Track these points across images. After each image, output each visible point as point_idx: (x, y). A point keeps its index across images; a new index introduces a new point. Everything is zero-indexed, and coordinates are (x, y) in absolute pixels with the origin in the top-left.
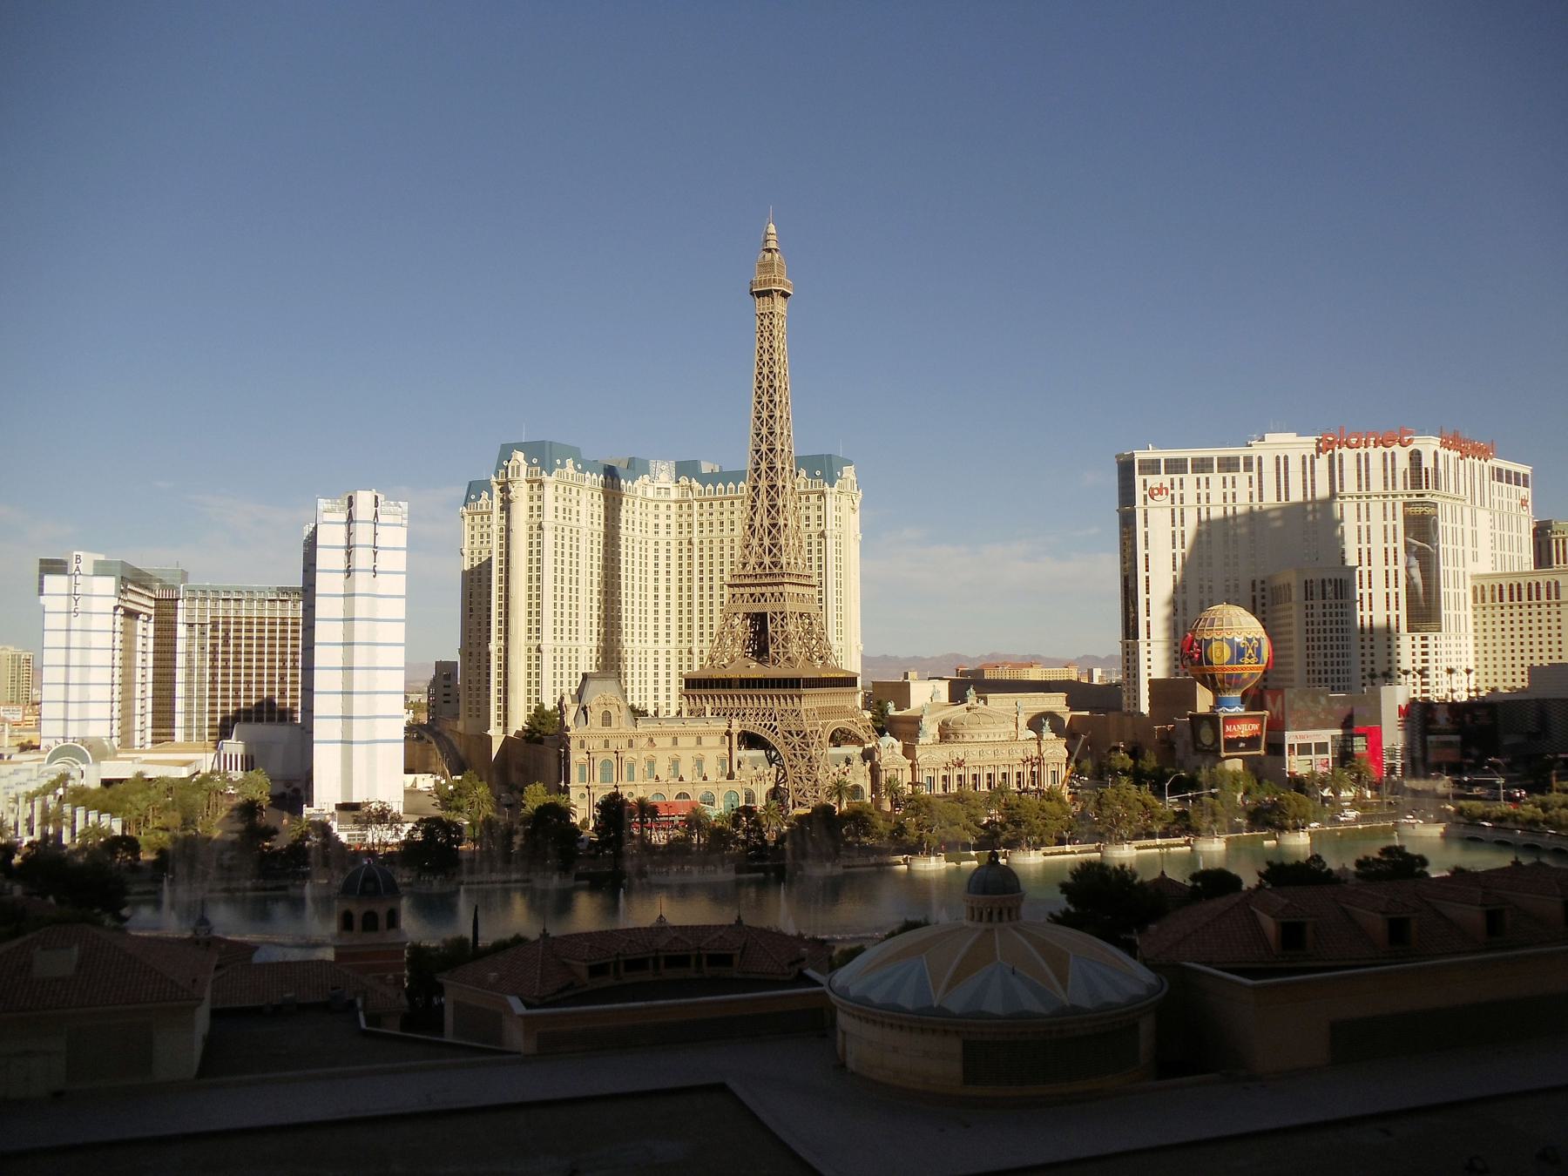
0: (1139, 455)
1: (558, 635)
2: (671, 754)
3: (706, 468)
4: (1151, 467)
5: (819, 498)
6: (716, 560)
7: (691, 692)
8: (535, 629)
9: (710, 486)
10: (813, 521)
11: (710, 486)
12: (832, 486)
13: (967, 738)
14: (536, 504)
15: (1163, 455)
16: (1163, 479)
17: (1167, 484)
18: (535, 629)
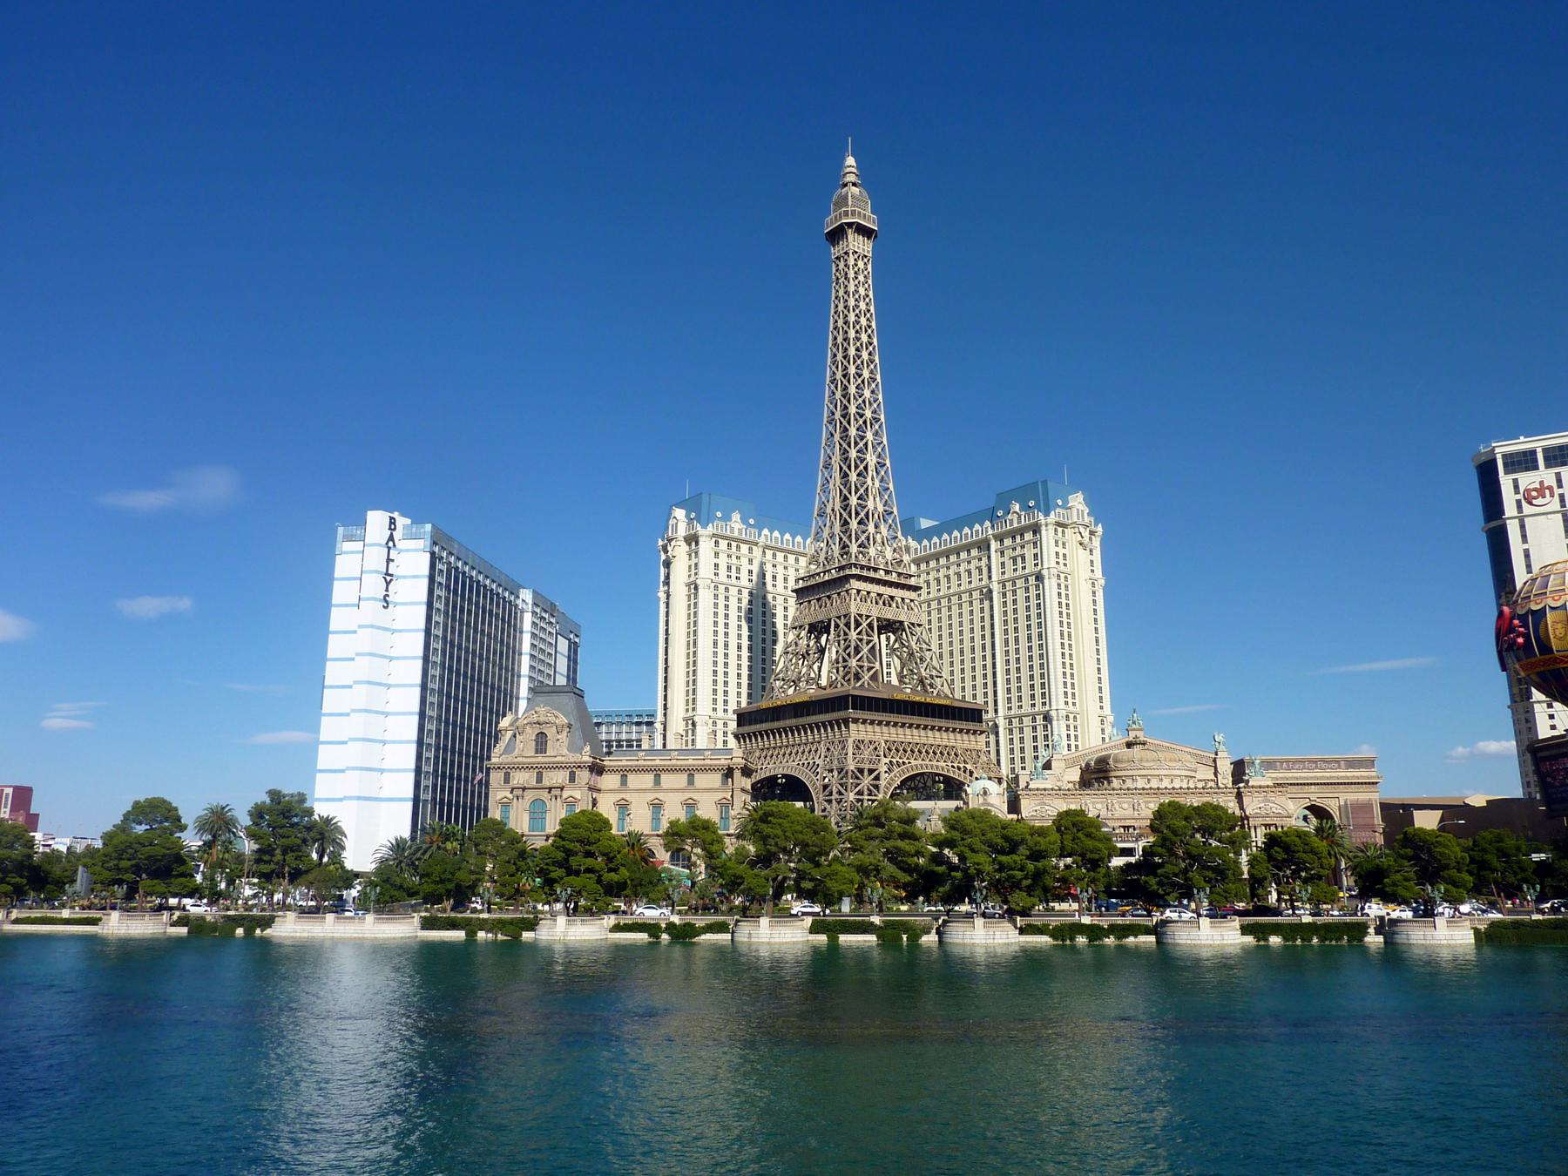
0: (1502, 449)
1: (720, 706)
2: (650, 796)
3: (925, 523)
4: (1525, 462)
5: (1035, 533)
6: (1024, 664)
7: (747, 729)
8: (692, 702)
9: (925, 542)
10: (1030, 561)
11: (925, 542)
12: (1047, 514)
13: (1116, 783)
14: (694, 560)
15: (1539, 444)
16: (1544, 475)
17: (1550, 480)
18: (692, 702)
